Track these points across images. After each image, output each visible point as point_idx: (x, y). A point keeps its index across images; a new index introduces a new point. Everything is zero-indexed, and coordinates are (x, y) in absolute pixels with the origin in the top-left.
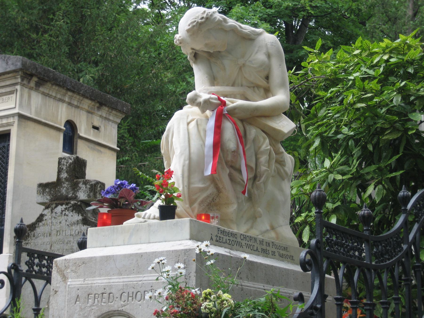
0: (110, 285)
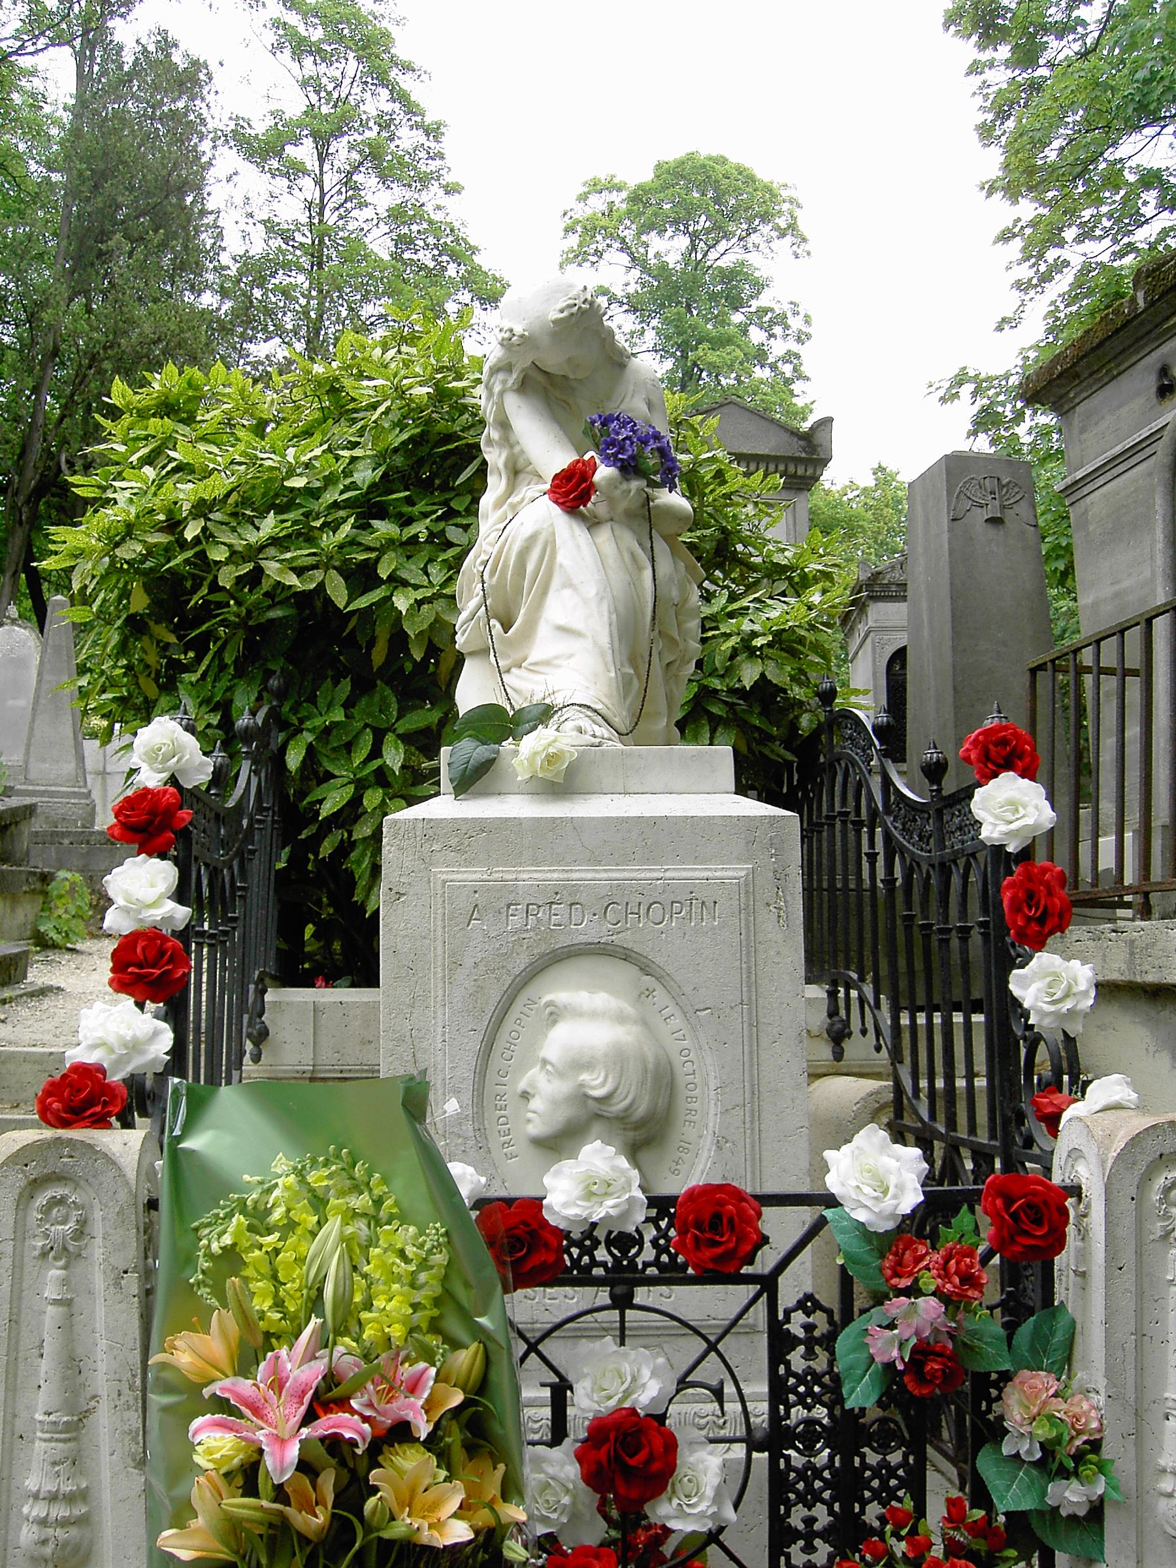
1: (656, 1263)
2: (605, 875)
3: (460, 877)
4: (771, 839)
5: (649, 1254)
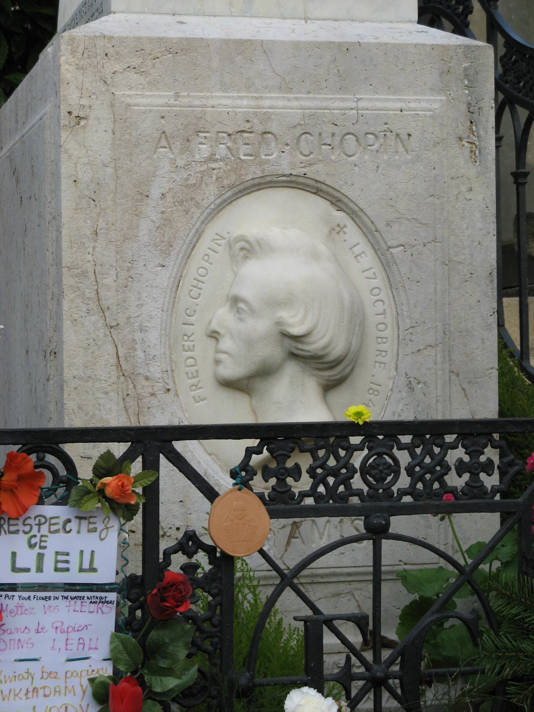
0: (264, 113)
1: (411, 491)
2: (295, 104)
3: (144, 101)
4: (465, 69)
5: (404, 481)
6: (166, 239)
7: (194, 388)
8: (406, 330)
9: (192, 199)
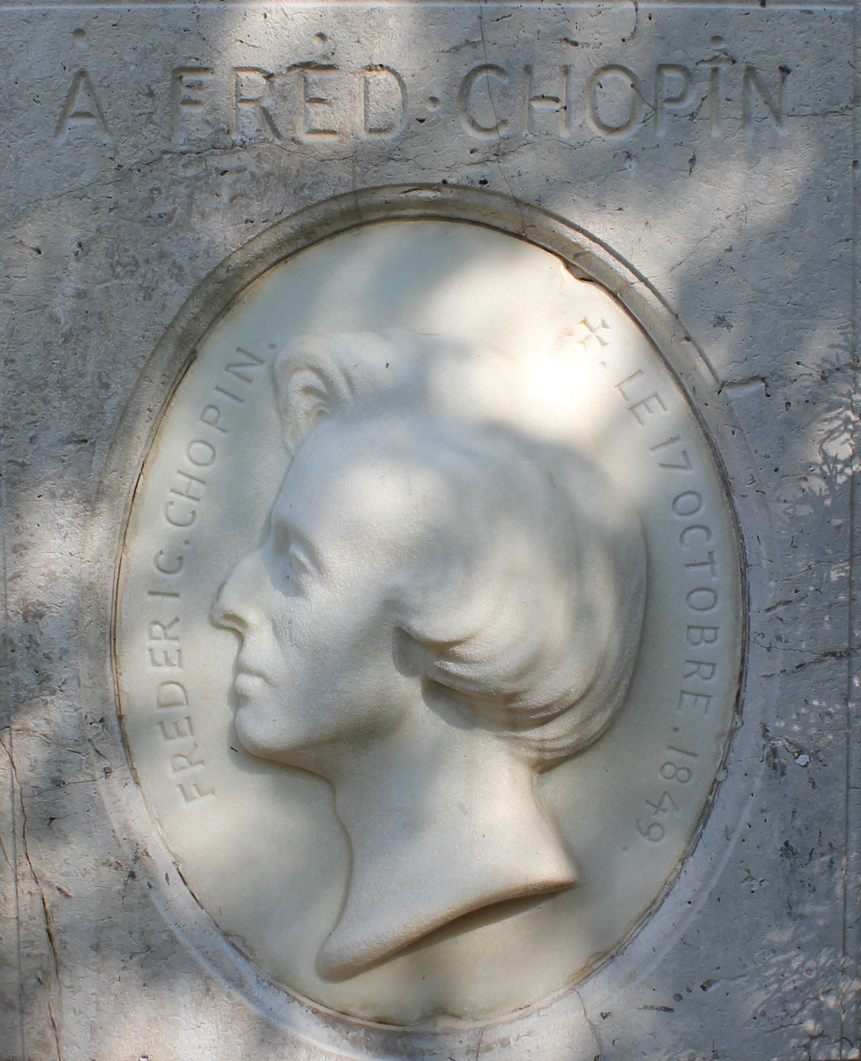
6: (90, 368)
7: (183, 761)
8: (768, 610)
9: (162, 256)
